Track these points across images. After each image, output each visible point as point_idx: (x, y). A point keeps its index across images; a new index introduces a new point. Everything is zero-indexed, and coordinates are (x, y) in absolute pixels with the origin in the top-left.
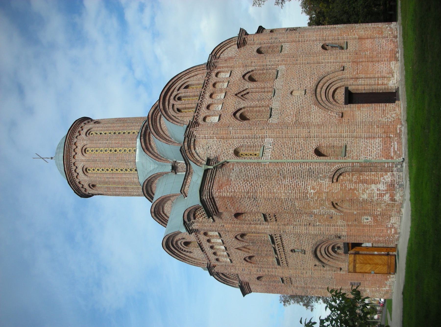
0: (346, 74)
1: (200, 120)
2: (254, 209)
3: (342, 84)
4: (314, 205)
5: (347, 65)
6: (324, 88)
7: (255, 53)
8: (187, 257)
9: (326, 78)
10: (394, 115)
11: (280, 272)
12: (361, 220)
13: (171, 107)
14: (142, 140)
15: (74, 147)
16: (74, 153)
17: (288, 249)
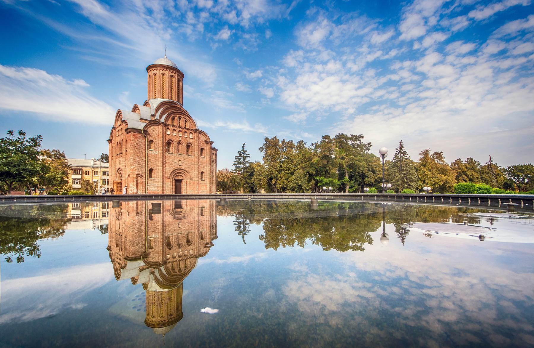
0: (188, 180)
5: (193, 180)
7: (201, 147)
11: (114, 155)
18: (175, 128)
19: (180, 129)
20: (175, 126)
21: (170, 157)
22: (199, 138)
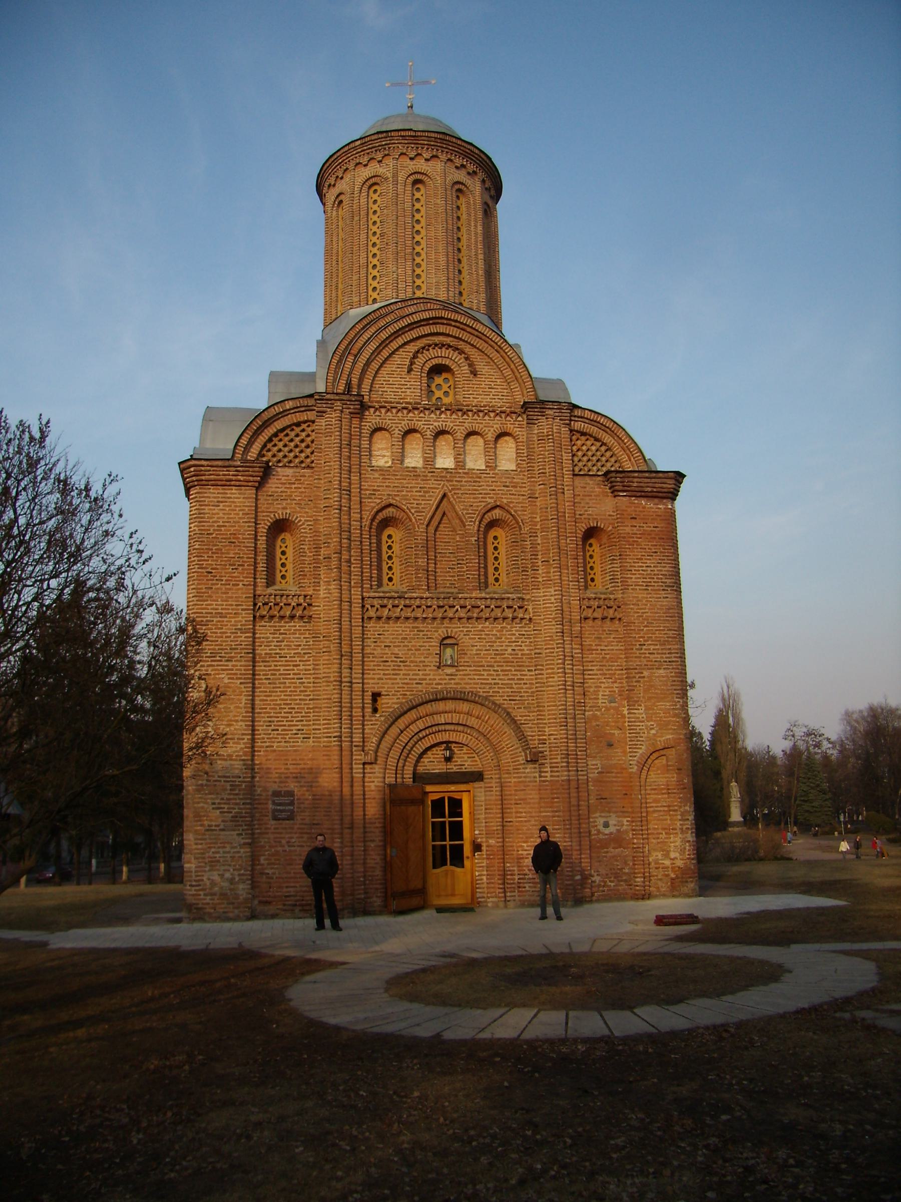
2: (633, 579)
4: (661, 709)
8: (385, 353)
12: (602, 812)
17: (456, 629)
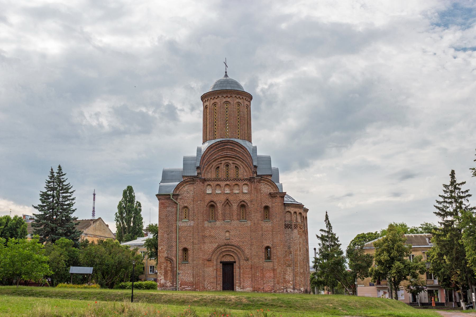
1: (208, 183)
3: (237, 260)
5: (250, 263)
6: (232, 250)
7: (264, 205)
9: (239, 251)
10: (209, 288)
13: (219, 163)
14: (217, 143)
15: (216, 97)
16: (213, 98)
18: (219, 183)
19: (228, 183)
20: (220, 180)
21: (212, 228)
22: (258, 190)
